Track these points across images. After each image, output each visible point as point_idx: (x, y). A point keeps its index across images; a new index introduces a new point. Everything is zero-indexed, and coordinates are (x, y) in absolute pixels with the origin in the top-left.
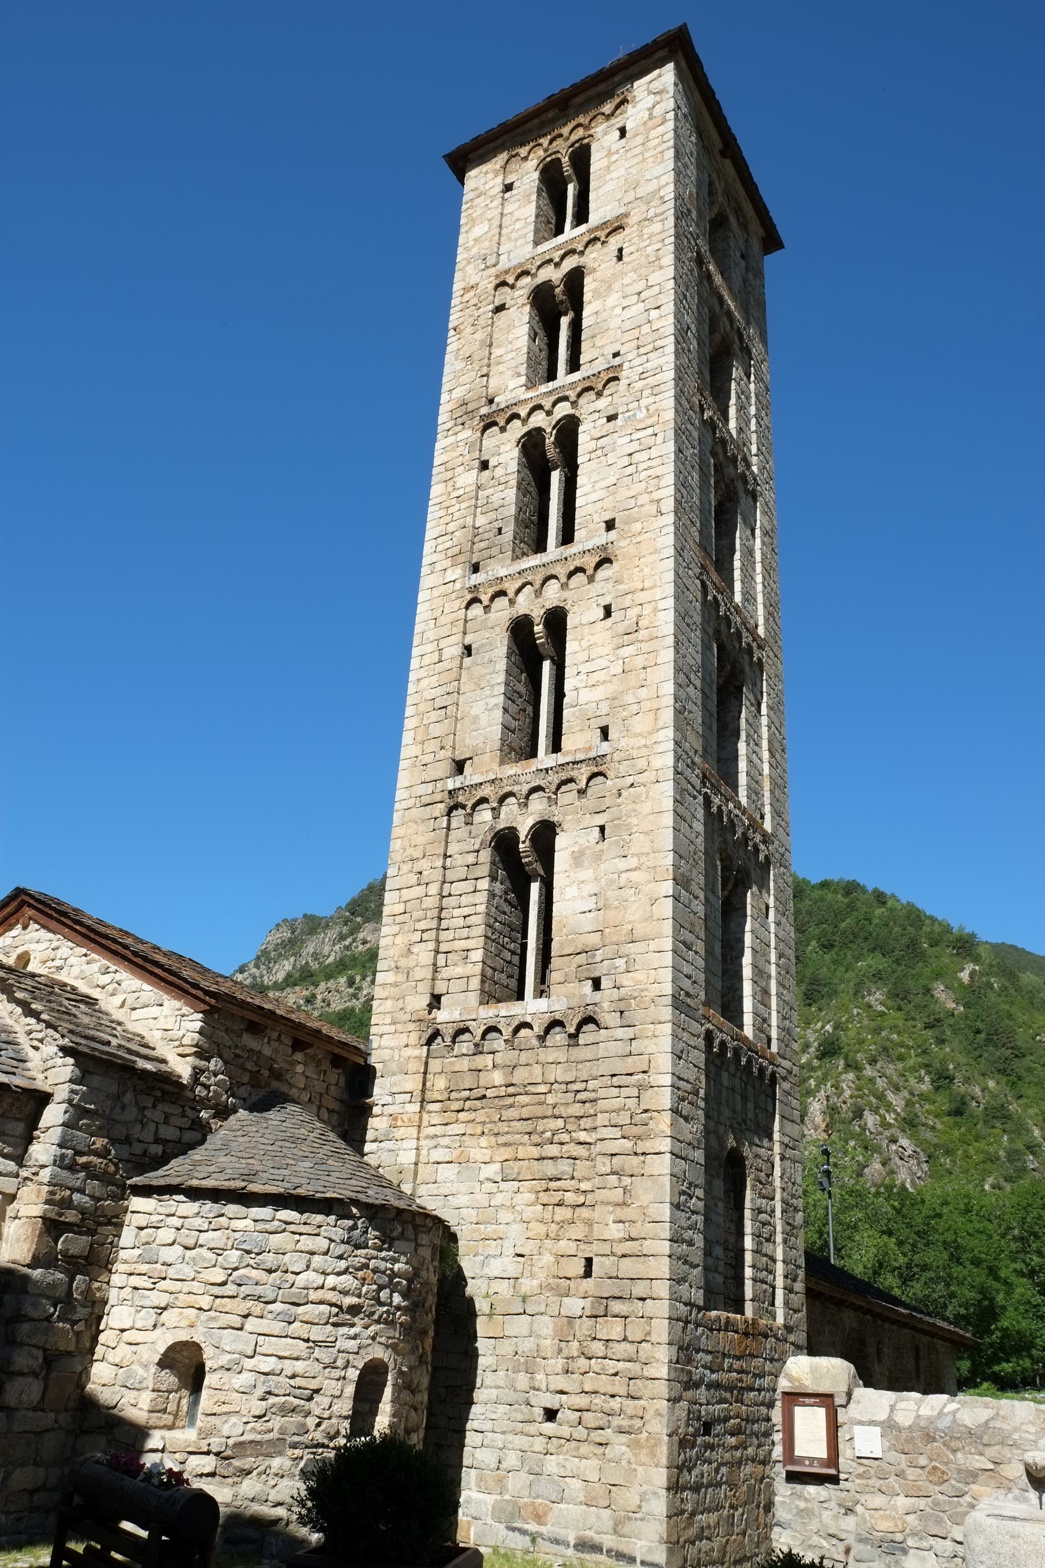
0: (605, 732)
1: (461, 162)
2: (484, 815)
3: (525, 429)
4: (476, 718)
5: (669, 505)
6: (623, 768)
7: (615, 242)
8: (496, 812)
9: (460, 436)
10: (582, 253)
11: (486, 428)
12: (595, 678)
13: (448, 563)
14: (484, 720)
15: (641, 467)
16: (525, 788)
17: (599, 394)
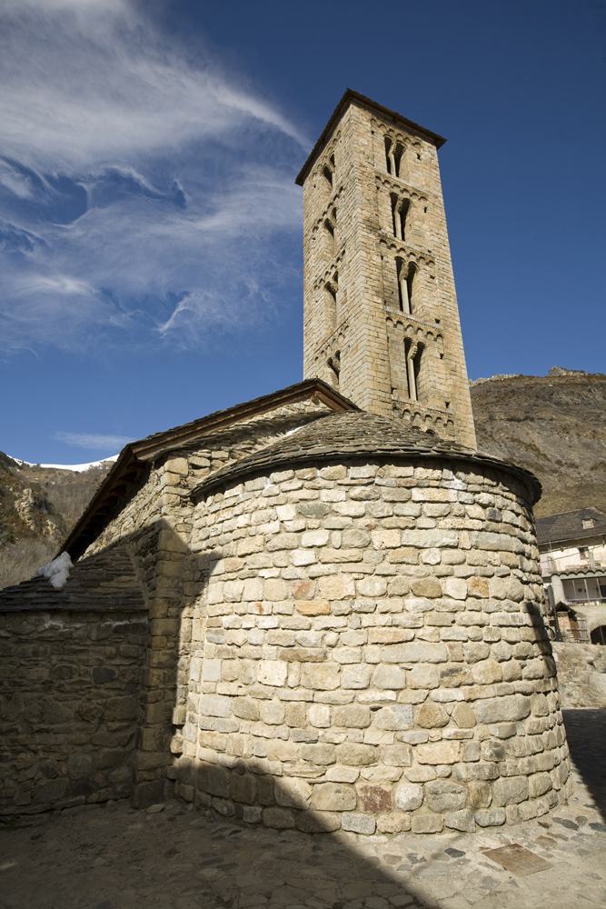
0: (447, 404)
1: (351, 97)
2: (407, 417)
3: (397, 255)
4: (396, 372)
5: (459, 328)
6: (459, 422)
7: (423, 203)
8: (413, 418)
9: (370, 236)
10: (411, 196)
11: (382, 241)
12: (442, 381)
13: (374, 293)
14: (399, 374)
15: (448, 307)
16: (425, 414)
17: (427, 264)
